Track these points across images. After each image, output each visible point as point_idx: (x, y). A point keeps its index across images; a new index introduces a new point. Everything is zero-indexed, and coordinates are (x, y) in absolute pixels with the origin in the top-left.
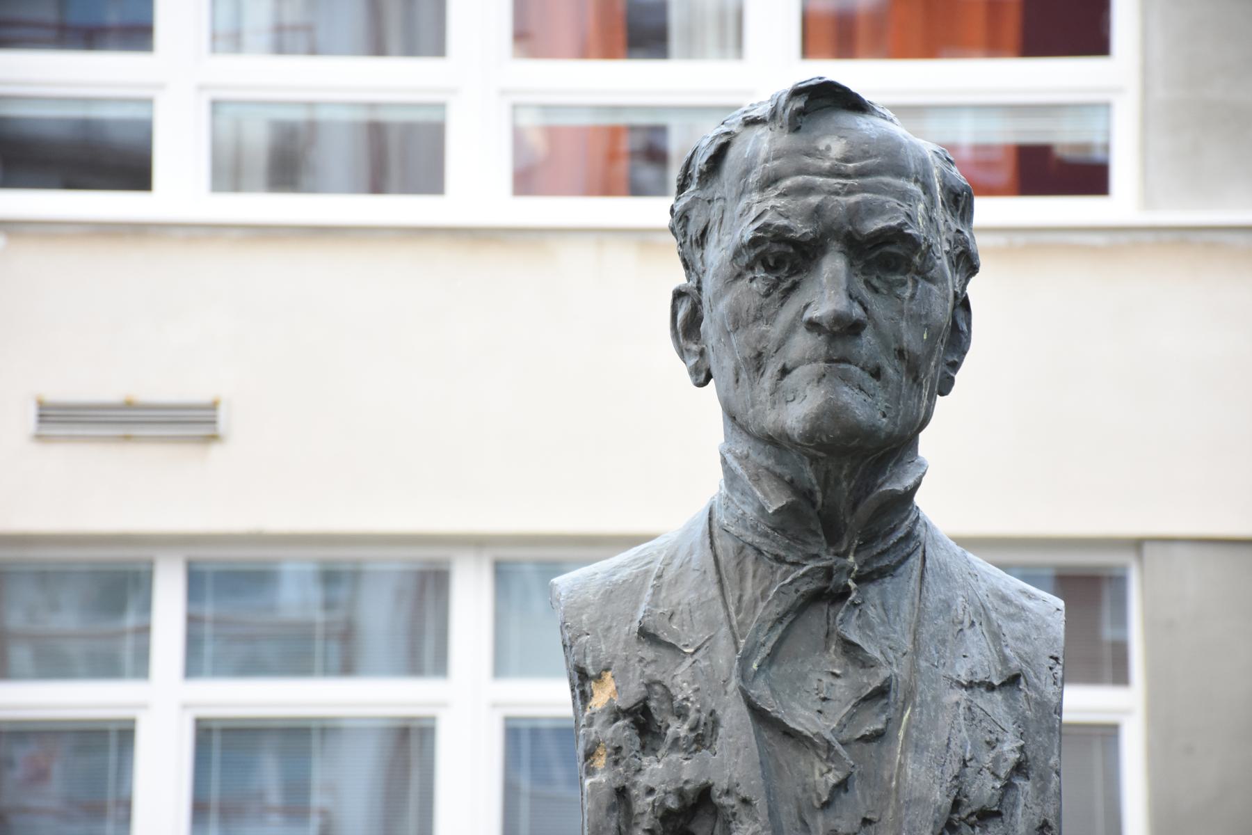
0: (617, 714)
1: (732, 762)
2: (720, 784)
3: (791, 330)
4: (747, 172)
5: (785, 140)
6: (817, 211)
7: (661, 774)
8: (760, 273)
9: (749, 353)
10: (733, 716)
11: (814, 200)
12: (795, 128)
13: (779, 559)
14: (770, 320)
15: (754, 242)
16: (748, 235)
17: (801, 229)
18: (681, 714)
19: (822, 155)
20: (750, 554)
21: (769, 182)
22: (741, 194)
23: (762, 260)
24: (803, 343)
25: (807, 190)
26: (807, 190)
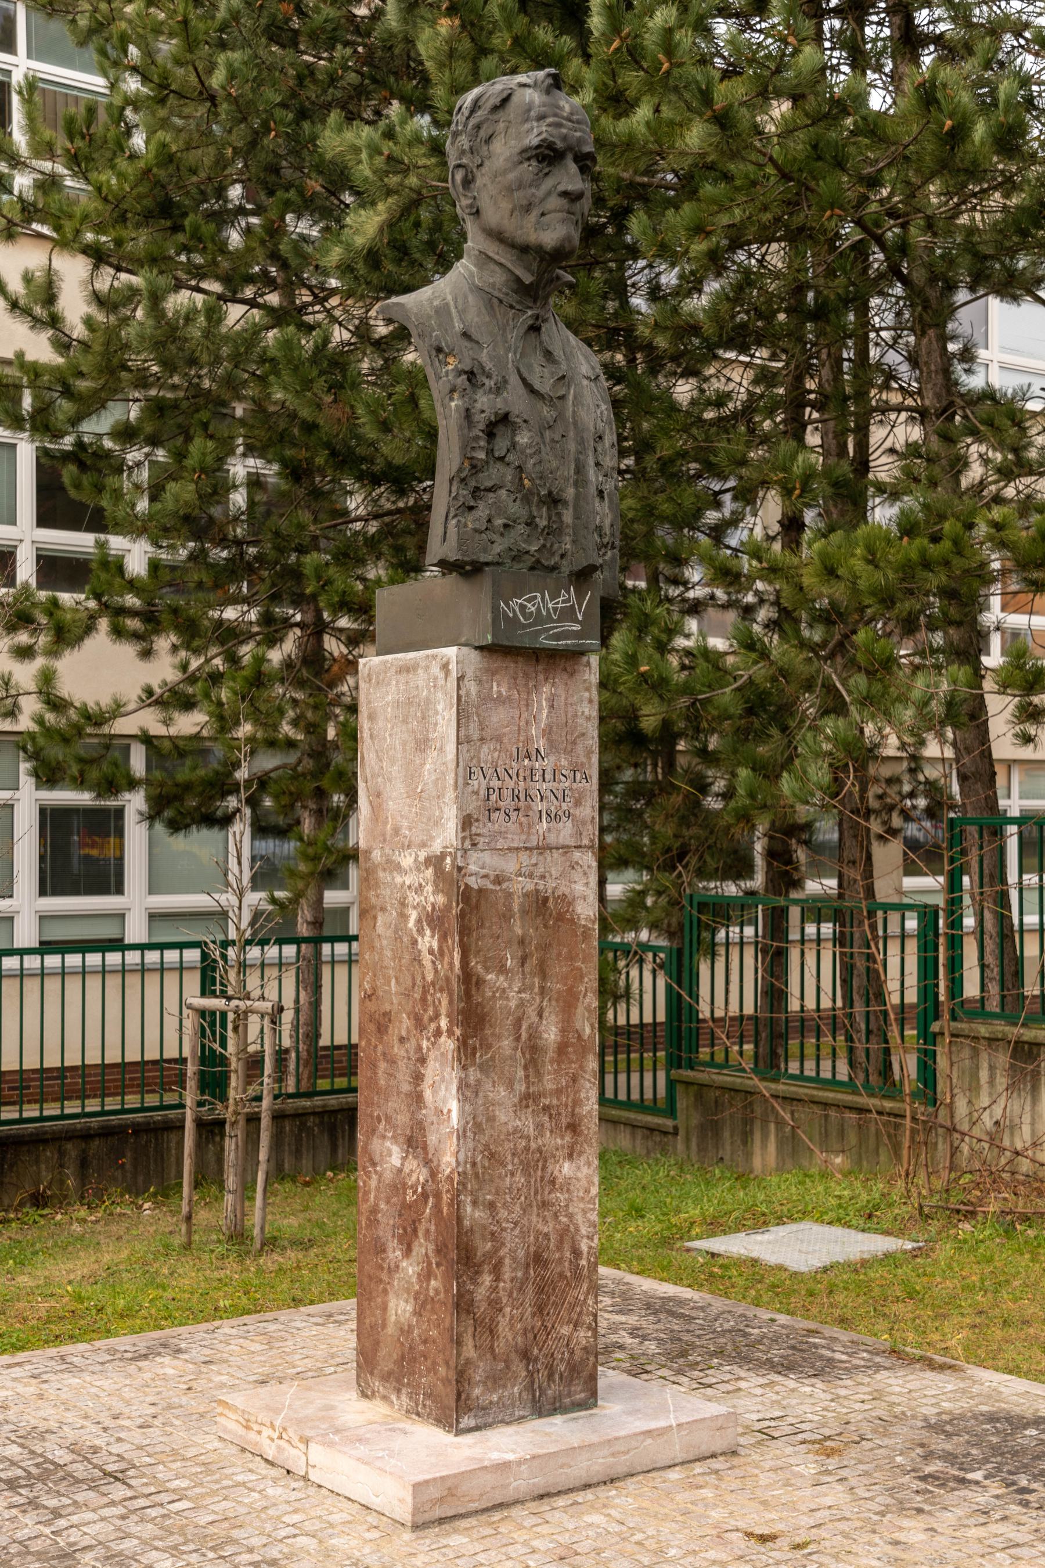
0: (460, 373)
1: (515, 400)
2: (515, 410)
3: (549, 193)
4: (529, 110)
5: (544, 98)
6: (565, 138)
7: (485, 403)
8: (534, 163)
9: (525, 202)
10: (514, 380)
11: (564, 131)
12: (548, 92)
13: (512, 307)
14: (537, 187)
15: (538, 147)
16: (535, 142)
17: (560, 145)
18: (489, 376)
19: (562, 109)
20: (495, 301)
21: (541, 118)
22: (527, 120)
23: (537, 156)
24: (555, 202)
25: (559, 125)
26: (559, 125)
